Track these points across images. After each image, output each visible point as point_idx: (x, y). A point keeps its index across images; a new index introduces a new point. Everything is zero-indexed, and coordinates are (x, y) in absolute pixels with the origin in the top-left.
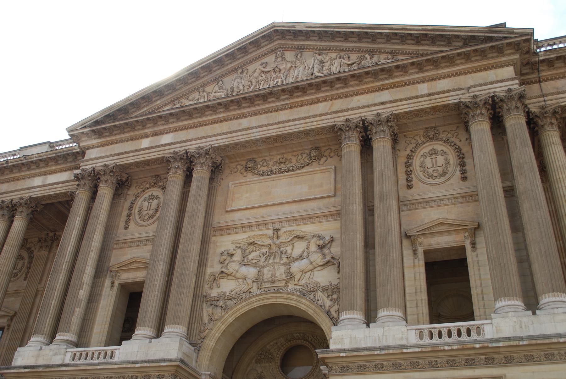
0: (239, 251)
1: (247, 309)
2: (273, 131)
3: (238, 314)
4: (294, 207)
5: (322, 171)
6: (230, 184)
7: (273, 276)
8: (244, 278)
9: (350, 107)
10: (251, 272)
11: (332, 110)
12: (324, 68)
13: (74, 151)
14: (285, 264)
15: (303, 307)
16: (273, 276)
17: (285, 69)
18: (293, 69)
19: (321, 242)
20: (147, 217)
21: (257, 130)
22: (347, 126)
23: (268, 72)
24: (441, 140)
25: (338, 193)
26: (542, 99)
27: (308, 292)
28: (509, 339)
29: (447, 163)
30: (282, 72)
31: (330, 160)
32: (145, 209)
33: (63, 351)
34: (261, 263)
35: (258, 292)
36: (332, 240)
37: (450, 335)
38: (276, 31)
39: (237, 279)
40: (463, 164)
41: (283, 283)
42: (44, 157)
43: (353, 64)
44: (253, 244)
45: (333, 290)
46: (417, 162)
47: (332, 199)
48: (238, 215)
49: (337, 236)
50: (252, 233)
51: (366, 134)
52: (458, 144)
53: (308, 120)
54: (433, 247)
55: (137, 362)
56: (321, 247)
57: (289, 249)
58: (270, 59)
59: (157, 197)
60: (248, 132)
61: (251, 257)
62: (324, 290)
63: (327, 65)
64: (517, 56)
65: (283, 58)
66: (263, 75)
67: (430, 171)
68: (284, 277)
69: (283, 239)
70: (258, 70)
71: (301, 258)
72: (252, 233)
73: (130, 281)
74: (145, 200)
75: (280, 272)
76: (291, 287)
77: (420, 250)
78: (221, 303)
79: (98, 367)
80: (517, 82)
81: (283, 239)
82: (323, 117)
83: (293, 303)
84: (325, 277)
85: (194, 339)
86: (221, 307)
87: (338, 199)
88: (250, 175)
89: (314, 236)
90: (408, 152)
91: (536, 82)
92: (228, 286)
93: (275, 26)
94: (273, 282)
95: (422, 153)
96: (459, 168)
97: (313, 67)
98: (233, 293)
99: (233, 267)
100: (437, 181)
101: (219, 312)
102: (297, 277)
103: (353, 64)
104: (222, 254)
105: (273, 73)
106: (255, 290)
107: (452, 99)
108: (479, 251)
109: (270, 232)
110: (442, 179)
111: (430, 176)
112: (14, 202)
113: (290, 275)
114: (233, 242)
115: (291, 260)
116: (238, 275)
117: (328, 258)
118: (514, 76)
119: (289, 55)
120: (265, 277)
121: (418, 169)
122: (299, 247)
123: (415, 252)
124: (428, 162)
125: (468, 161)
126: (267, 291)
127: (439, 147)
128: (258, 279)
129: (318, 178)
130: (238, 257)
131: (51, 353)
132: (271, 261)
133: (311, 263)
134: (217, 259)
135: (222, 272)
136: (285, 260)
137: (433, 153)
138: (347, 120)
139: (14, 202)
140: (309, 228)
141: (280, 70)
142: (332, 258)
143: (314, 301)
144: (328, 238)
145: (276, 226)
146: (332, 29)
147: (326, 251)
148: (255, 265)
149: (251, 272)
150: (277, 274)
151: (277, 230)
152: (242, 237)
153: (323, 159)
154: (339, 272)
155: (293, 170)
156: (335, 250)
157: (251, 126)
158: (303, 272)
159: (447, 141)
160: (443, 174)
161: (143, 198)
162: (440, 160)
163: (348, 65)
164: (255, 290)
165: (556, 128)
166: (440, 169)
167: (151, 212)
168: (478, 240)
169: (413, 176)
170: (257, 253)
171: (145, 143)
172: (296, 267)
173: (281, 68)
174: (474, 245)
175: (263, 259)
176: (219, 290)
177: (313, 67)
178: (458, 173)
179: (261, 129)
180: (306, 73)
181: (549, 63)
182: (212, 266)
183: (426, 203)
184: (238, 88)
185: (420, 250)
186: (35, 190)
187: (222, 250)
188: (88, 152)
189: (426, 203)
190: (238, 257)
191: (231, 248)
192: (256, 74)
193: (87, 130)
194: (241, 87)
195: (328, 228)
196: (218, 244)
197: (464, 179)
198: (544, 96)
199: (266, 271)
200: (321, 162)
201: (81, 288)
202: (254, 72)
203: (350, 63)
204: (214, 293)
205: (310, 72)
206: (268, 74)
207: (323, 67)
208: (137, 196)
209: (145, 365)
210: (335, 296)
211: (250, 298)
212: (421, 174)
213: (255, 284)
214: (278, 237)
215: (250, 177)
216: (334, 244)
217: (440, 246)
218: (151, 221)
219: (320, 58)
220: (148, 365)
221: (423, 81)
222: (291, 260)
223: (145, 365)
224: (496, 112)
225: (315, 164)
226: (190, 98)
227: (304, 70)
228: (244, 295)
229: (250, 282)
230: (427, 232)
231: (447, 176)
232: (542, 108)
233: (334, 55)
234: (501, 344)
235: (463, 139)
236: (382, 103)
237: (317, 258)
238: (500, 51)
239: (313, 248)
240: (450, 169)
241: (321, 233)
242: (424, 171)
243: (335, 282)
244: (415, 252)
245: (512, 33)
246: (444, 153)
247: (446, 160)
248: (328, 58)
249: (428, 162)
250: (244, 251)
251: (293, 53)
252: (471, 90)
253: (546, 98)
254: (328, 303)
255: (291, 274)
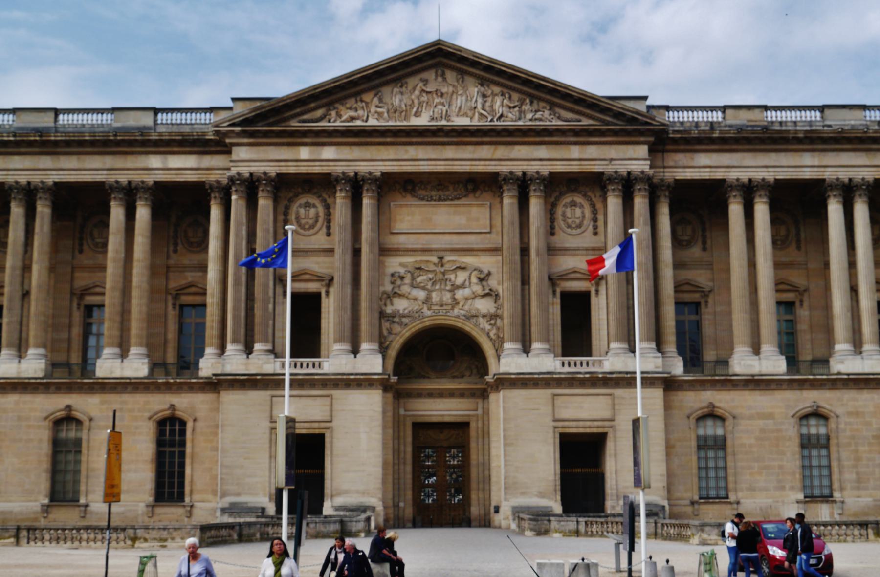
0: (409, 275)
1: (420, 326)
2: (441, 167)
3: (413, 330)
4: (455, 237)
5: (478, 205)
6: (392, 204)
7: (441, 299)
8: (415, 299)
9: (512, 156)
10: (421, 294)
11: (495, 157)
12: (488, 104)
13: (207, 137)
14: (450, 291)
15: (467, 329)
16: (441, 299)
17: (447, 93)
18: (454, 96)
19: (482, 276)
20: (307, 226)
21: (426, 163)
22: (510, 178)
23: (430, 92)
24: (580, 193)
25: (494, 230)
26: (662, 170)
27: (470, 317)
28: (620, 373)
29: (584, 217)
30: (445, 96)
31: (485, 194)
32: (303, 217)
33: (272, 360)
34: (429, 287)
35: (429, 313)
36: (489, 274)
37: (582, 365)
38: (440, 50)
39: (408, 299)
40: (595, 220)
41: (450, 307)
42: (167, 138)
43: (514, 107)
44: (420, 269)
45: (493, 317)
46: (559, 210)
47: (488, 235)
48: (402, 239)
49: (493, 270)
50: (419, 258)
51: (523, 185)
52: (594, 199)
53: (474, 163)
54: (567, 289)
55: (352, 374)
56: (481, 280)
57: (452, 276)
58: (430, 75)
59: (314, 206)
60: (416, 163)
61: (419, 280)
62: (484, 316)
63: (489, 99)
64: (652, 139)
65: (445, 79)
66: (424, 95)
67: (570, 221)
68: (450, 301)
69: (447, 267)
70: (418, 87)
71: (462, 286)
72: (419, 258)
73: (302, 290)
74: (300, 206)
75: (447, 297)
76: (456, 311)
77: (558, 290)
78: (397, 319)
79: (316, 377)
80: (648, 162)
81: (447, 267)
82: (487, 163)
83: (459, 325)
84: (484, 306)
85: (383, 350)
86: (398, 323)
87: (493, 236)
88: (409, 196)
89: (475, 270)
90: (553, 199)
91: (660, 152)
92: (400, 305)
93: (439, 44)
94: (442, 306)
95: (564, 203)
96: (592, 223)
97: (476, 101)
98: (406, 311)
99: (405, 289)
100: (574, 232)
101: (397, 328)
102: (461, 304)
103: (514, 107)
104: (393, 275)
105: (434, 95)
106: (425, 310)
107: (597, 168)
108: (600, 296)
109: (435, 259)
110: (579, 231)
111: (569, 226)
112: (133, 185)
113: (455, 302)
114: (402, 265)
115: (455, 288)
116: (410, 296)
117: (487, 291)
118: (647, 157)
119: (450, 75)
120: (434, 300)
121: (560, 218)
122: (461, 277)
123: (554, 292)
124: (569, 212)
125: (601, 218)
126: (437, 313)
127: (579, 199)
128: (428, 300)
129: (475, 211)
130: (407, 280)
131: (261, 362)
132: (437, 287)
133: (474, 293)
134: (388, 279)
135: (395, 293)
136: (448, 288)
137: (573, 204)
138: (511, 173)
139: (133, 185)
140: (469, 260)
141: (442, 95)
142: (491, 290)
143: (477, 325)
144: (486, 272)
145: (441, 254)
146: (499, 67)
147: (484, 283)
148: (424, 288)
149: (421, 294)
150: (445, 299)
151: (441, 258)
152: (409, 260)
153: (478, 193)
154: (495, 302)
155: (452, 200)
156: (493, 283)
157: (420, 157)
158: (467, 299)
159: (585, 196)
160: (579, 226)
161: (297, 204)
162: (578, 211)
163: (510, 107)
164: (425, 310)
165: (668, 201)
166: (578, 221)
167: (311, 222)
168: (600, 288)
169: (556, 224)
170: (424, 277)
171: (304, 152)
172: (460, 294)
173: (444, 90)
174: (597, 291)
175: (430, 284)
176: (393, 308)
177: (476, 101)
178: (591, 227)
179: (430, 163)
180: (469, 104)
181: (675, 141)
182: (383, 285)
183: (565, 250)
184: (400, 107)
185: (558, 290)
186: (157, 172)
187: (390, 270)
188: (235, 149)
189: (565, 250)
190: (407, 280)
191: (402, 271)
192: (417, 92)
193: (238, 129)
194: (403, 106)
195: (486, 263)
196: (386, 264)
197: (596, 234)
198: (664, 167)
199: (434, 295)
200: (477, 195)
201: (269, 303)
202: (414, 89)
203: (512, 105)
204: (389, 310)
205: (473, 105)
206: (430, 95)
207: (485, 102)
208: (291, 200)
209: (358, 377)
210: (493, 322)
211: (424, 318)
212: (562, 223)
213: (425, 306)
214: (442, 266)
215: (410, 200)
216: (491, 277)
217: (573, 289)
218: (312, 231)
219: (482, 89)
220: (362, 377)
221: (576, 143)
222: (455, 288)
223: (358, 377)
224: (628, 185)
225: (471, 196)
226: (348, 105)
227: (467, 100)
228: (417, 315)
229: (420, 303)
230: (565, 276)
231: (583, 228)
232: (662, 180)
233: (497, 89)
234: (614, 376)
235: (598, 194)
236: (541, 160)
237: (478, 289)
238: (641, 133)
239: (474, 280)
240: (586, 222)
241: (480, 266)
242: (564, 221)
243: (493, 310)
244: (554, 292)
245: (654, 120)
246: (582, 206)
247: (583, 213)
248: (489, 92)
249: (569, 212)
250: (412, 275)
251: (455, 74)
252: (613, 162)
253: (666, 170)
254: (488, 327)
255: (455, 299)
